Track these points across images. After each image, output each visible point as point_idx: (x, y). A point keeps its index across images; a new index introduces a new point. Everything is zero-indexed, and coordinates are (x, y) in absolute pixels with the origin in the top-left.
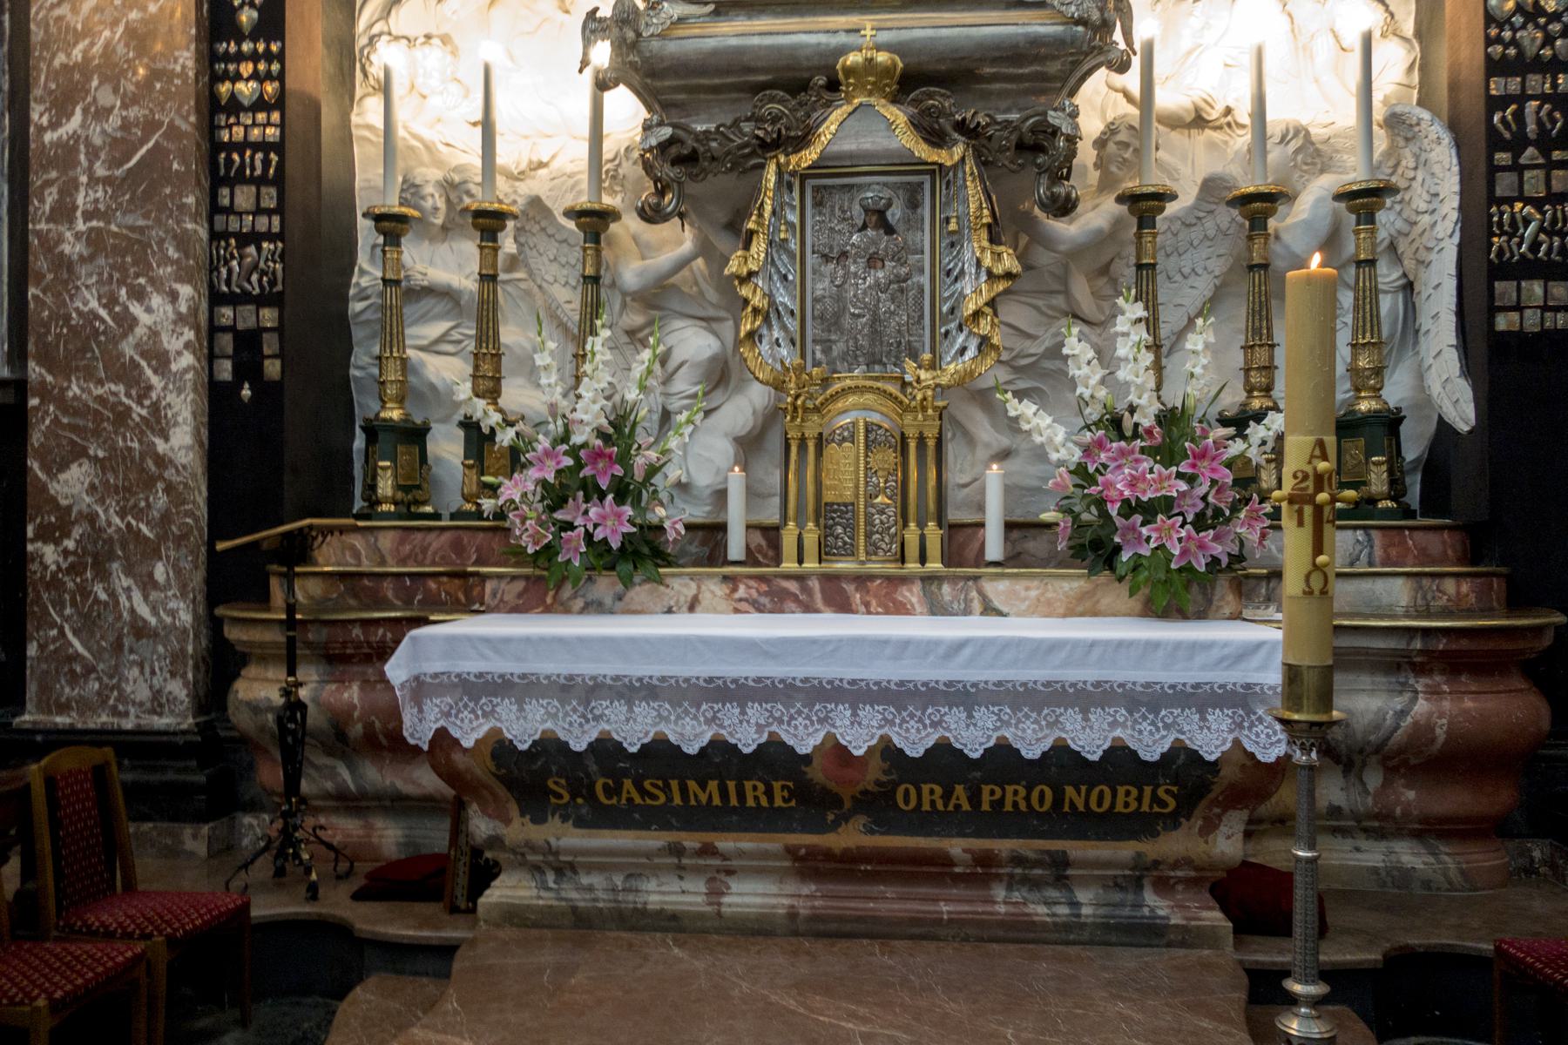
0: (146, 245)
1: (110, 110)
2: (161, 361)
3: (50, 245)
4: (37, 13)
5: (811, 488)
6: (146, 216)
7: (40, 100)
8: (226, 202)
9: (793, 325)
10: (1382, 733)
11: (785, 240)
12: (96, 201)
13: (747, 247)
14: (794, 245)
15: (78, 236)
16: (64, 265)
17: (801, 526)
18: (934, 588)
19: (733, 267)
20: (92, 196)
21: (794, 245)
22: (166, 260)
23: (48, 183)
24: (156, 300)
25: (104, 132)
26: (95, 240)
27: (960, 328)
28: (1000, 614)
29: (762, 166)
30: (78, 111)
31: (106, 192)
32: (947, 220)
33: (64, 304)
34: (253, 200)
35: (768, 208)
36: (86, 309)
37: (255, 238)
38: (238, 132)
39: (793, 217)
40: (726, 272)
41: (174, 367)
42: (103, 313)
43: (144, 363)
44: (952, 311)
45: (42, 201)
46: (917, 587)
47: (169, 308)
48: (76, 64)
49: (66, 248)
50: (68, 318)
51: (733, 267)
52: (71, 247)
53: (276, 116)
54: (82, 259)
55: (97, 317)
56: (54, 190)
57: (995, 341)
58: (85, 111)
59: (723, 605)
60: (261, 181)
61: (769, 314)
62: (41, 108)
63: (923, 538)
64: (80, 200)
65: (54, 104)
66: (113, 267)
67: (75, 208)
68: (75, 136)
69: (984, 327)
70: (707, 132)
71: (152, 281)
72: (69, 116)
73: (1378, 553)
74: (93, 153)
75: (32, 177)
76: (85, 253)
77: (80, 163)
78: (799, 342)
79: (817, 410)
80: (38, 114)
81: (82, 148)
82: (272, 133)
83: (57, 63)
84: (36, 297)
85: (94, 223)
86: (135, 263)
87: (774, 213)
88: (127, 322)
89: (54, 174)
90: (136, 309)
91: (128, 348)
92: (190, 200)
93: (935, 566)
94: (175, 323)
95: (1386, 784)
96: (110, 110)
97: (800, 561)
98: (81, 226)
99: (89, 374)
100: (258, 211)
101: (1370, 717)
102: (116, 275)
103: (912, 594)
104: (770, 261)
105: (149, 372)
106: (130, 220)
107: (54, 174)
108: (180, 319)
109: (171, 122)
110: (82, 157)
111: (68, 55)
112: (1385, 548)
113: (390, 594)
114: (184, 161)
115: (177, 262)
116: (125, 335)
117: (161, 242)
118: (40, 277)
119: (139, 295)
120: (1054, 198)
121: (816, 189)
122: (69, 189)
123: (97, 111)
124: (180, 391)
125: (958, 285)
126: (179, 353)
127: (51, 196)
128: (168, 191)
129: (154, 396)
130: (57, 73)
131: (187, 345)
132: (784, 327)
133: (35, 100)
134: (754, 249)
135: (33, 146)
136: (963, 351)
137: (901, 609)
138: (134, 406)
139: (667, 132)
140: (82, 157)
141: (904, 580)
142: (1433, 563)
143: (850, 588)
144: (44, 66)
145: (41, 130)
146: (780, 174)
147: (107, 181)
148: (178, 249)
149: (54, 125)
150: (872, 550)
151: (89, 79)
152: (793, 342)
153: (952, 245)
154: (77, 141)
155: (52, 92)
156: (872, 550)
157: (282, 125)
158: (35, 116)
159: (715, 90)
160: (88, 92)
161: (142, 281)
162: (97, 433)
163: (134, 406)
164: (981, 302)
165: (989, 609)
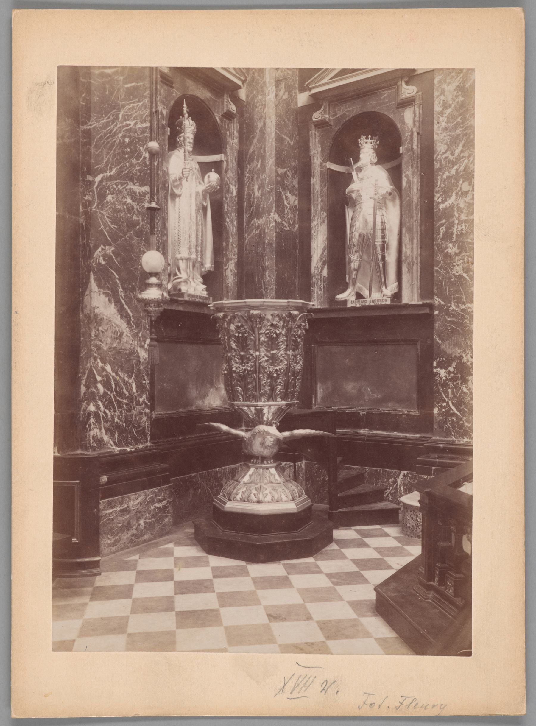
4: (437, 157)
12: (462, 230)
20: (460, 228)
23: (442, 225)
30: (454, 194)
31: (466, 226)
33: (449, 273)
36: (457, 274)
48: (453, 175)
49: (449, 250)
54: (456, 254)
56: (444, 227)
58: (457, 194)
62: (439, 195)
64: (455, 231)
67: (453, 234)
72: (450, 197)
76: (457, 252)
77: (455, 215)
80: (438, 197)
81: (455, 209)
83: (445, 176)
84: (437, 271)
89: (444, 221)
107: (444, 221)
111: (449, 172)
123: (462, 193)
127: (442, 230)
130: (445, 180)
133: (436, 192)
140: (456, 213)
145: (439, 203)
149: (444, 201)
151: (458, 181)
154: (453, 206)
155: (443, 188)
158: (436, 198)
160: (458, 186)
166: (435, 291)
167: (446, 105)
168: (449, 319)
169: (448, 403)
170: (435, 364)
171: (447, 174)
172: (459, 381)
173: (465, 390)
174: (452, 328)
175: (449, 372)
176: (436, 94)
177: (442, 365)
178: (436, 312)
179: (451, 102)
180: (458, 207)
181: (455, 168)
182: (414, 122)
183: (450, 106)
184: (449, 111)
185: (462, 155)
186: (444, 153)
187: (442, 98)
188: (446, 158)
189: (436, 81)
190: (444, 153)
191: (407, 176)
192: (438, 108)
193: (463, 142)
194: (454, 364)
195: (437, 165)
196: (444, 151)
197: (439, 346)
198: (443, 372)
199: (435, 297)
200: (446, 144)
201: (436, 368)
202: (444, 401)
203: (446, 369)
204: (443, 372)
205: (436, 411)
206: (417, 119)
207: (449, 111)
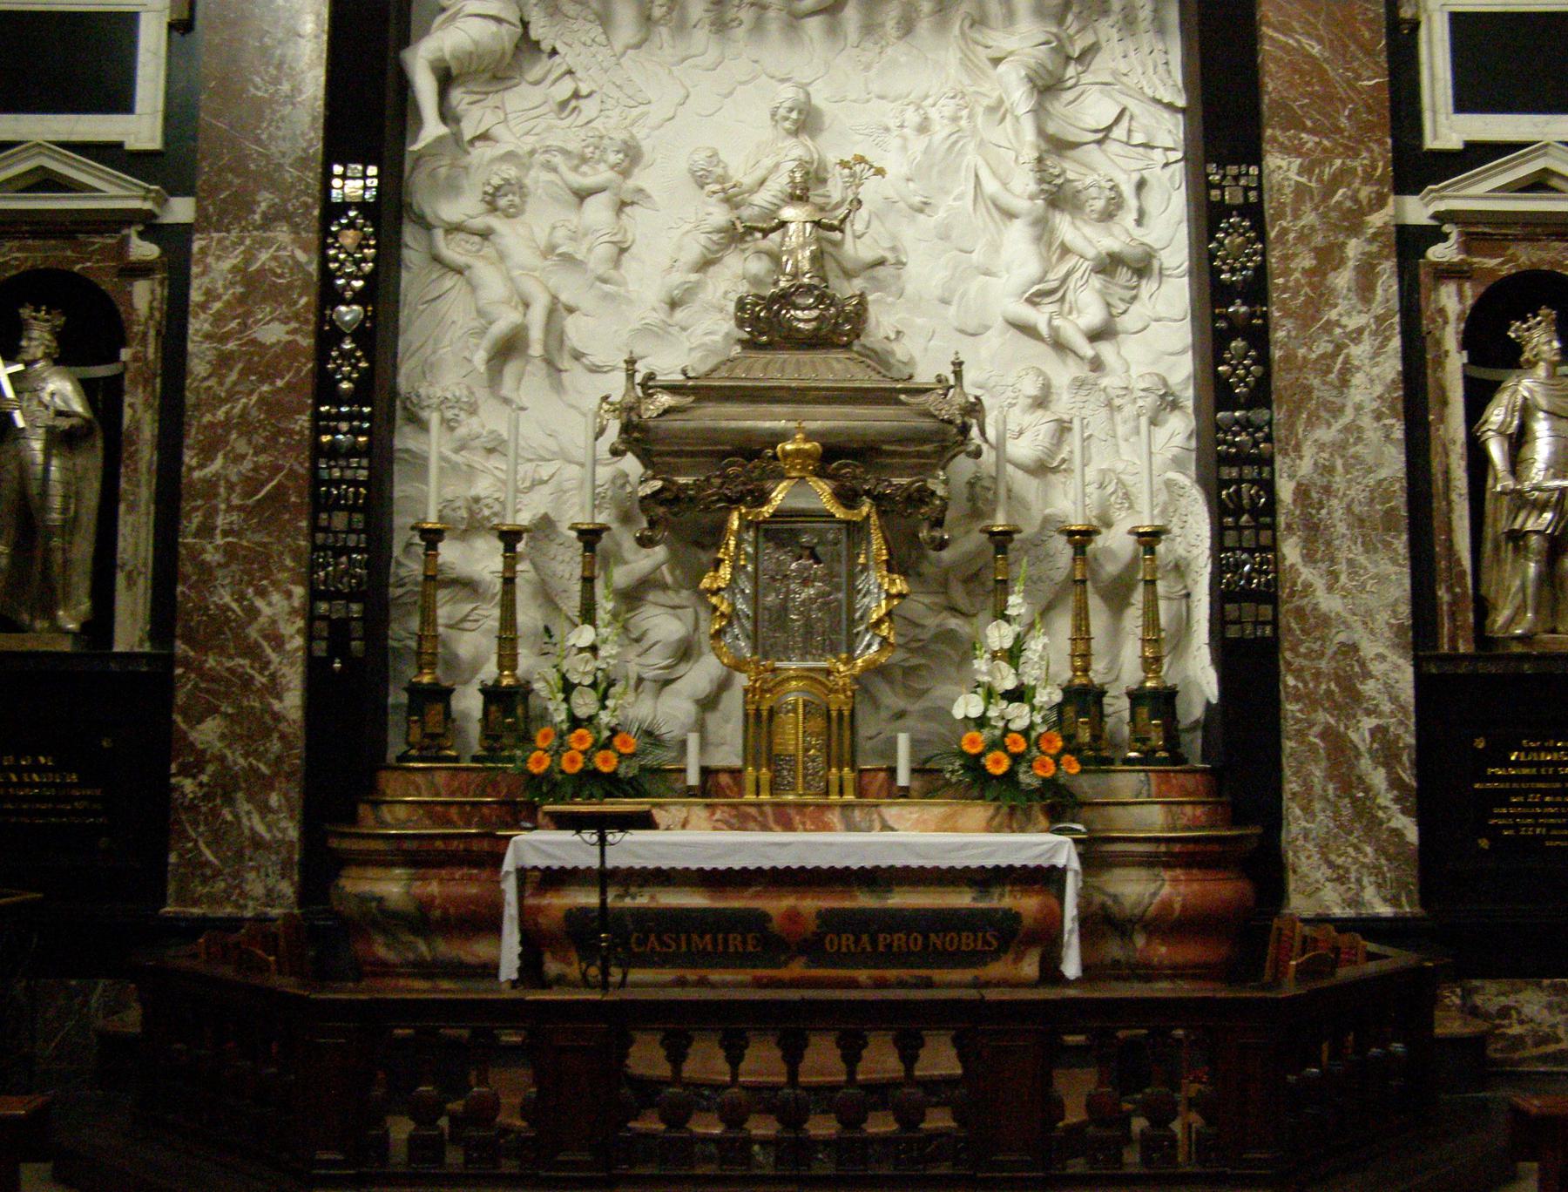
0: (269, 556)
1: (243, 457)
2: (278, 642)
3: (195, 555)
5: (764, 743)
6: (269, 535)
7: (191, 448)
8: (324, 523)
9: (748, 625)
10: (1141, 908)
11: (744, 566)
12: (231, 523)
13: (716, 569)
14: (750, 568)
15: (217, 548)
16: (206, 569)
17: (757, 768)
18: (848, 812)
19: (706, 583)
21: (750, 568)
22: (283, 568)
24: (276, 597)
25: (239, 473)
26: (230, 552)
27: (867, 630)
28: (892, 829)
29: (729, 510)
30: (220, 456)
32: (858, 555)
33: (205, 599)
34: (346, 522)
35: (732, 543)
37: (347, 551)
38: (337, 473)
39: (750, 550)
40: (702, 586)
41: (288, 647)
42: (234, 605)
43: (265, 644)
44: (862, 618)
45: (190, 522)
46: (837, 811)
47: (285, 603)
49: (207, 557)
50: (207, 608)
51: (706, 583)
52: (211, 556)
53: (365, 462)
54: (220, 565)
55: (230, 609)
57: (892, 640)
58: (226, 456)
59: (705, 824)
60: (352, 509)
61: (732, 617)
63: (841, 779)
64: (220, 521)
65: (202, 450)
66: (243, 571)
68: (217, 474)
69: (885, 629)
70: (687, 485)
71: (273, 583)
72: (212, 460)
73: (1154, 788)
74: (231, 487)
75: (183, 504)
78: (754, 638)
79: (769, 691)
80: (189, 458)
81: (222, 483)
82: (363, 475)
85: (230, 539)
86: (261, 569)
87: (737, 546)
88: (253, 613)
89: (199, 502)
90: (260, 603)
91: (253, 633)
92: (304, 524)
93: (849, 797)
94: (290, 613)
95: (1148, 943)
96: (243, 457)
97: (758, 794)
98: (219, 541)
99: (222, 650)
100: (351, 530)
101: (1134, 897)
102: (246, 578)
103: (834, 817)
104: (733, 580)
105: (268, 651)
106: (258, 537)
107: (199, 502)
108: (294, 612)
109: (291, 469)
110: (222, 490)
112: (1158, 786)
113: (455, 818)
114: (300, 495)
115: (292, 569)
116: (249, 624)
117: (282, 553)
118: (186, 578)
119: (262, 593)
120: (933, 539)
121: (767, 531)
122: (212, 513)
124: (292, 665)
125: (866, 600)
126: (292, 637)
127: (197, 519)
128: (287, 517)
129: (272, 668)
130: (205, 427)
131: (299, 631)
132: (742, 626)
134: (721, 572)
135: (184, 481)
136: (869, 646)
137: (826, 827)
138: (257, 675)
139: (658, 484)
140: (222, 490)
141: (829, 806)
142: (1189, 794)
143: (792, 812)
144: (195, 423)
145: (191, 469)
146: (741, 517)
147: (241, 508)
148: (294, 559)
149: (201, 466)
150: (808, 786)
151: (229, 433)
152: (748, 637)
153: (862, 572)
156: (808, 786)
157: (369, 468)
158: (186, 459)
159: (692, 454)
160: (227, 443)
161: (265, 582)
162: (227, 695)
163: (257, 675)
164: (883, 611)
165: (886, 827)
166: (178, 630)
167: (210, 295)
168: (203, 685)
169: (196, 842)
170: (174, 768)
171: (208, 418)
172: (218, 801)
173: (229, 818)
174: (208, 702)
175: (201, 785)
176: (195, 270)
177: (185, 771)
178: (179, 671)
179: (221, 291)
180: (228, 481)
181: (224, 409)
182: (151, 308)
183: (219, 297)
184: (217, 306)
185: (238, 388)
186: (205, 379)
187: (206, 280)
188: (210, 388)
189: (196, 247)
190: (205, 379)
191: (132, 406)
192: (196, 296)
193: (240, 366)
194: (210, 768)
195: (190, 398)
196: (205, 374)
197: (184, 735)
198: (188, 785)
199: (178, 643)
200: (209, 362)
201: (174, 775)
202: (189, 839)
203: (194, 777)
204: (188, 785)
205: (173, 858)
206: (156, 304)
207: (217, 306)
